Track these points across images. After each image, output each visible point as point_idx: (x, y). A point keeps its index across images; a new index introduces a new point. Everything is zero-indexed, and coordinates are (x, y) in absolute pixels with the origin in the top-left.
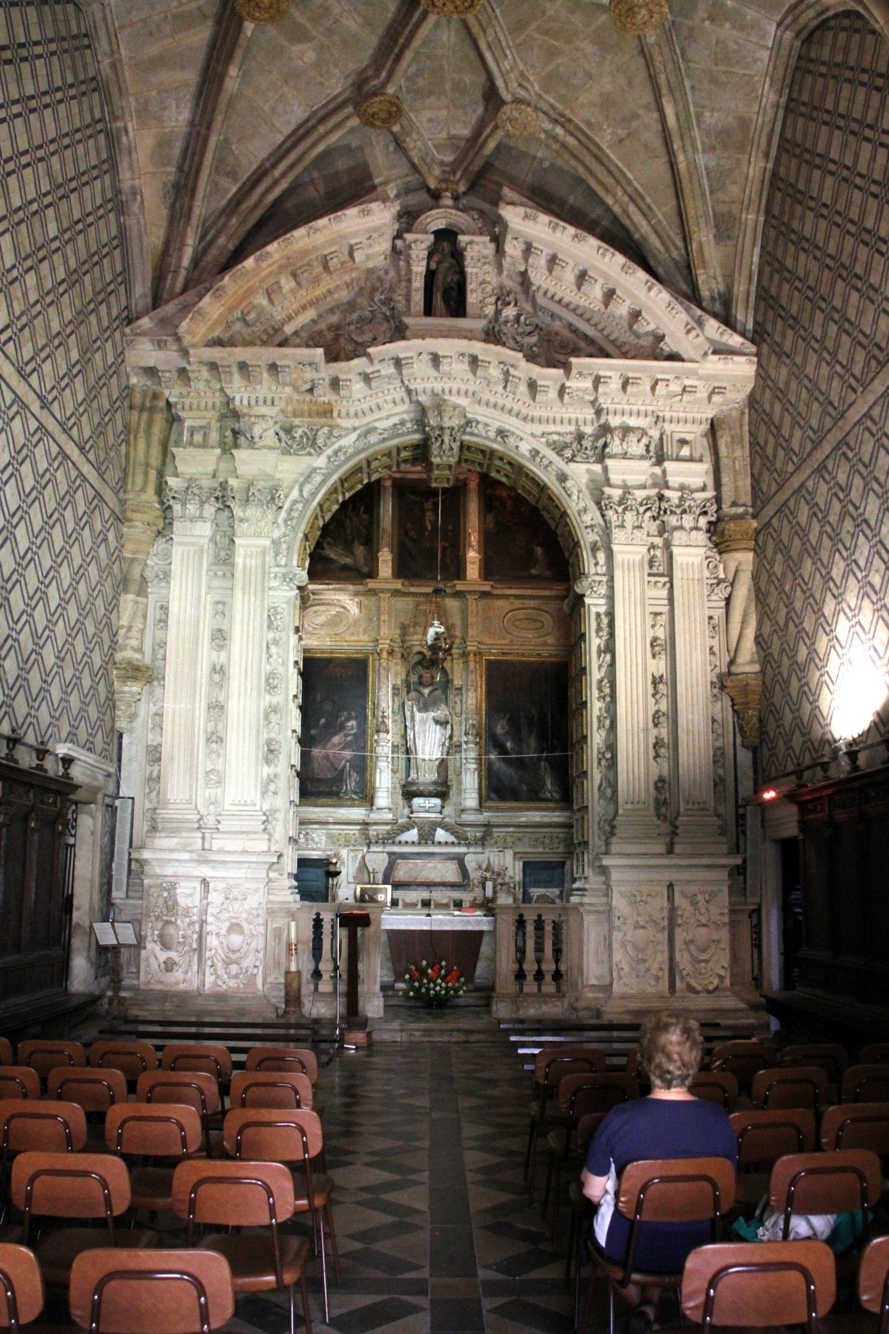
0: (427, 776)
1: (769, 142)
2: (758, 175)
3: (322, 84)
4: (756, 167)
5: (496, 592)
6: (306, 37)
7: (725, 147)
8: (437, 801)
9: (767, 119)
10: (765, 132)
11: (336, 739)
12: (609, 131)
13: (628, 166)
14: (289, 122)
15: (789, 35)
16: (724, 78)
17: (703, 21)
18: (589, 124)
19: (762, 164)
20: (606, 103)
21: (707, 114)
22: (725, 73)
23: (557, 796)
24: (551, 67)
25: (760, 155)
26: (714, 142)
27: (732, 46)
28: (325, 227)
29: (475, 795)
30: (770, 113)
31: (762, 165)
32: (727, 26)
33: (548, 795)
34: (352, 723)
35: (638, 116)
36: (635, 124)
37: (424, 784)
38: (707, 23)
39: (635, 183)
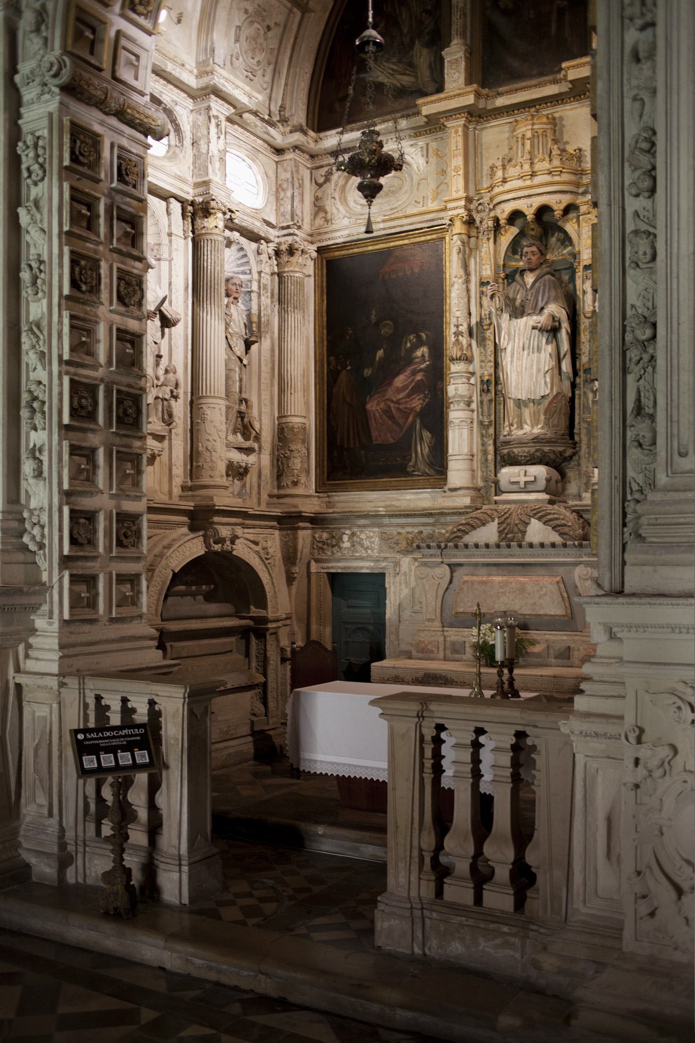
0: (528, 428)
8: (539, 471)
34: (423, 351)
37: (521, 443)
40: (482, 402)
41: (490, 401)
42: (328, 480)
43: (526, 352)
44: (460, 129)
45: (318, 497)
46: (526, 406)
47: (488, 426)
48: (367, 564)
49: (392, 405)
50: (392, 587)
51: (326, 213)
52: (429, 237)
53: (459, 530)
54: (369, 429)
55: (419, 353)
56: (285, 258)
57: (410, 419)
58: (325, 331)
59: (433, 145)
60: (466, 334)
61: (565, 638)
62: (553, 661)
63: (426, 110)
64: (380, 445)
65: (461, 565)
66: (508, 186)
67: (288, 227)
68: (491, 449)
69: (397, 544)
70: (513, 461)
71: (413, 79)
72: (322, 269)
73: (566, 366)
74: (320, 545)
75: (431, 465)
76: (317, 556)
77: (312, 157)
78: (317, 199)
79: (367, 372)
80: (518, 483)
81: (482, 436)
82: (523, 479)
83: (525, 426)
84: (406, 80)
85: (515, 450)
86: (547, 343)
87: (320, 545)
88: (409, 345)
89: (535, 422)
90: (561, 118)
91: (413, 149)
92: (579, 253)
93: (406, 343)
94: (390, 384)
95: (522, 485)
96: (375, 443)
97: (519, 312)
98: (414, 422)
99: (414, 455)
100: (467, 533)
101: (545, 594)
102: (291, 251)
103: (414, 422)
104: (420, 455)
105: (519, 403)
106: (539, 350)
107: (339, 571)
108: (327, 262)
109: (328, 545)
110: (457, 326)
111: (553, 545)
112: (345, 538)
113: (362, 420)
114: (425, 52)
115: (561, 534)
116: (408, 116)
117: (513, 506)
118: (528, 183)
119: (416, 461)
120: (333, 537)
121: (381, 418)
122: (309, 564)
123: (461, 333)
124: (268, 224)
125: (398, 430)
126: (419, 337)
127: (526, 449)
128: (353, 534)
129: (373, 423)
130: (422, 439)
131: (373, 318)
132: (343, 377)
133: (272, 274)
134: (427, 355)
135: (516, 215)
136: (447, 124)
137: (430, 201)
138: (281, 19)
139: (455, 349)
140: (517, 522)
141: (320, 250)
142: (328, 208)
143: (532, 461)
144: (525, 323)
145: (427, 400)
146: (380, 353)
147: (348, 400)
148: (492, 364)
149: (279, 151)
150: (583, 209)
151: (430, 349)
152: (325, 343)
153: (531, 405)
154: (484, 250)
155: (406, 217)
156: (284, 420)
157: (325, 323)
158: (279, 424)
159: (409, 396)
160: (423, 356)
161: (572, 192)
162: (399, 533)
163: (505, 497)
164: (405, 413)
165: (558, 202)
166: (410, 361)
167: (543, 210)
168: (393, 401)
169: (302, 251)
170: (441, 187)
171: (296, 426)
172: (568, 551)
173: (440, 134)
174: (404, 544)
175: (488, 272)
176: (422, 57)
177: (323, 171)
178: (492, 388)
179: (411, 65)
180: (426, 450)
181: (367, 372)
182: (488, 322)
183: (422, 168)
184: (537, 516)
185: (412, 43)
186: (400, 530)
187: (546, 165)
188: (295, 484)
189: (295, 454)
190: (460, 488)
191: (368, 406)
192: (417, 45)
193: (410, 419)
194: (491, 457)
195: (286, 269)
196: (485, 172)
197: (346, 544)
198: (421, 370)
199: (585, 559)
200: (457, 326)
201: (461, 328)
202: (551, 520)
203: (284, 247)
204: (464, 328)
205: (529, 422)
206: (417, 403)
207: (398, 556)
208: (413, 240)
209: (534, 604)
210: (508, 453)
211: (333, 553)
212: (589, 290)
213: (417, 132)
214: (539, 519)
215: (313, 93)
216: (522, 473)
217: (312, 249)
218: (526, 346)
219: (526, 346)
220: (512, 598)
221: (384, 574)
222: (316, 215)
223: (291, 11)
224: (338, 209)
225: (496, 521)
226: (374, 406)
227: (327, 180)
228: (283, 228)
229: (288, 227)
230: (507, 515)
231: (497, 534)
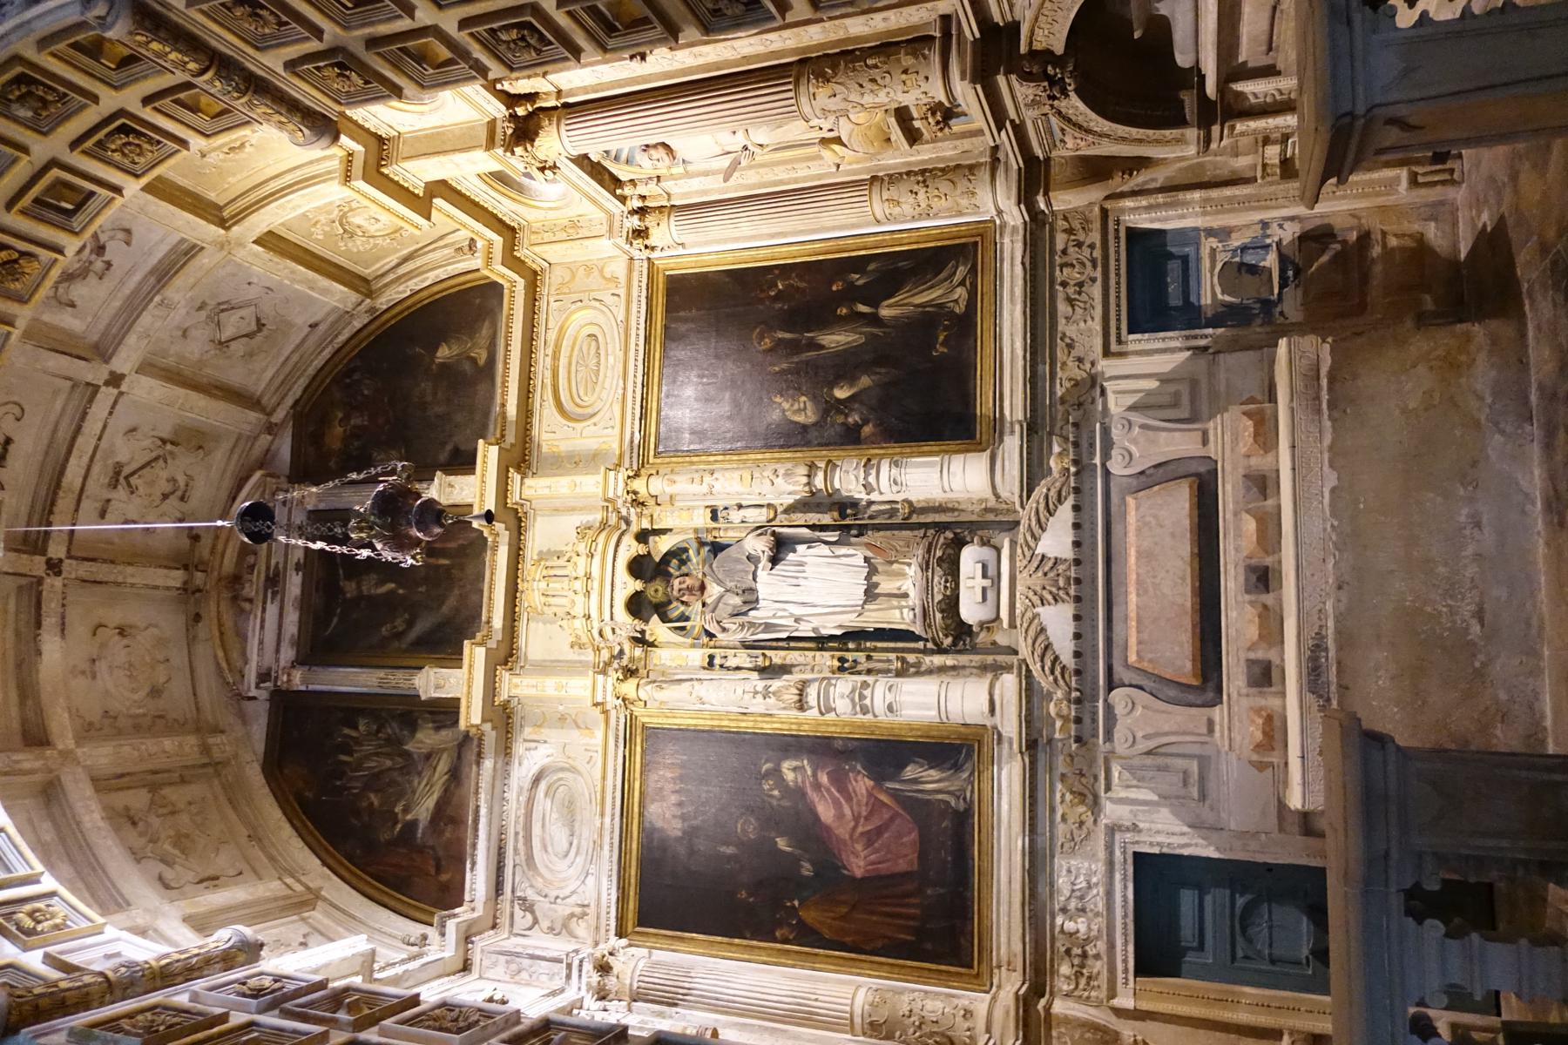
0: (907, 590)
5: (511, 438)
8: (970, 558)
11: (826, 812)
23: (962, 271)
29: (957, 461)
33: (961, 293)
37: (928, 588)
40: (869, 672)
41: (869, 658)
42: (972, 967)
43: (801, 582)
44: (516, 680)
45: (999, 987)
46: (876, 585)
47: (903, 660)
48: (1118, 886)
49: (860, 829)
50: (1160, 839)
51: (573, 915)
52: (639, 749)
53: (1052, 672)
54: (892, 876)
55: (790, 776)
56: (611, 982)
57: (884, 798)
58: (737, 941)
59: (528, 732)
60: (769, 682)
61: (1229, 487)
62: (1270, 502)
63: (476, 719)
64: (919, 857)
65: (1109, 669)
66: (594, 614)
67: (569, 966)
68: (938, 660)
69: (1082, 823)
70: (951, 604)
71: (445, 756)
72: (647, 934)
73: (832, 536)
74: (1083, 981)
75: (957, 768)
76: (1103, 994)
77: (494, 927)
78: (551, 929)
79: (807, 869)
80: (984, 590)
81: (918, 674)
82: (980, 582)
83: (904, 588)
84: (443, 766)
85: (938, 597)
86: (794, 551)
87: (1083, 981)
88: (776, 793)
89: (903, 575)
90: (540, 553)
91: (525, 762)
92: (696, 531)
93: (772, 796)
94: (828, 829)
95: (987, 583)
96: (915, 867)
97: (748, 597)
98: (888, 792)
99: (940, 797)
100: (1056, 658)
101: (1155, 517)
102: (604, 968)
103: (888, 792)
104: (941, 785)
105: (871, 594)
106: (801, 564)
107: (1131, 948)
108: (640, 924)
109: (1082, 966)
110: (756, 693)
111: (1076, 508)
112: (1070, 926)
113: (878, 887)
114: (419, 735)
115: (1060, 501)
116: (480, 755)
117: (1019, 588)
118: (596, 585)
119: (948, 793)
120: (1068, 952)
121: (877, 851)
122: (1119, 1012)
123: (767, 688)
124: (553, 994)
125: (897, 822)
126: (767, 775)
127: (936, 579)
128: (1064, 910)
129: (884, 868)
130: (915, 781)
131: (730, 850)
132: (810, 916)
133: (630, 1010)
134: (795, 763)
135: (636, 605)
136: (504, 696)
137: (593, 741)
138: (305, 929)
139: (786, 697)
140: (1040, 574)
141: (620, 934)
142: (568, 911)
143: (952, 567)
144: (768, 583)
145: (859, 767)
146: (782, 843)
147: (844, 910)
148: (818, 654)
149: (466, 967)
150: (646, 524)
151: (787, 758)
152: (755, 943)
153: (875, 579)
154: (669, 663)
155: (604, 778)
156: (858, 1020)
157: (725, 940)
158: (864, 1034)
159: (849, 799)
160: (794, 769)
161: (623, 534)
162: (1064, 818)
163: (1004, 614)
164: (876, 806)
165: (630, 548)
166: (799, 793)
167: (638, 567)
168: (854, 828)
169: (611, 954)
170: (580, 722)
171: (870, 998)
172: (1086, 487)
173: (516, 719)
174: (1082, 809)
175: (698, 656)
176: (426, 738)
177: (518, 913)
178: (850, 656)
179: (428, 757)
180: (934, 774)
181: (807, 869)
182: (761, 659)
183: (550, 751)
184: (1032, 544)
185: (408, 755)
186: (1058, 817)
187: (582, 561)
188: (968, 1014)
189: (917, 1006)
190: (991, 695)
191: (859, 873)
192: (408, 747)
193: (884, 798)
194: (949, 660)
195: (628, 982)
196: (576, 658)
197: (1080, 925)
198: (815, 775)
199: (1097, 460)
200: (756, 693)
201: (759, 688)
202: (1039, 521)
203: (596, 978)
204: (760, 685)
205: (898, 584)
206: (862, 784)
207: (1104, 821)
208: (638, 775)
209: (1173, 535)
210: (942, 611)
211: (1097, 957)
212: (742, 512)
213: (505, 751)
214: (1036, 539)
215: (418, 915)
216: (970, 583)
217: (615, 942)
218: (795, 581)
219: (795, 581)
220: (1163, 574)
221: (1136, 854)
222: (572, 935)
223: (303, 919)
224: (573, 892)
225: (1039, 610)
226: (858, 863)
227: (528, 907)
228: (569, 977)
229: (569, 966)
230: (1031, 594)
231: (1060, 605)
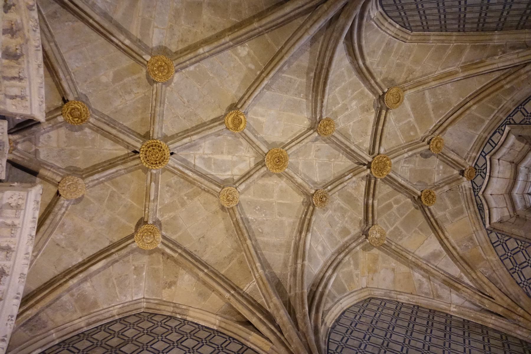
1: (95, 322)
2: (76, 327)
3: (86, 81)
4: (81, 323)
6: (114, 81)
7: (76, 301)
9: (104, 315)
10: (98, 317)
12: (62, 237)
13: (44, 253)
14: (70, 58)
15: (144, 305)
16: (110, 285)
17: (133, 265)
18: (63, 224)
19: (83, 324)
20: (78, 232)
21: (89, 284)
22: (113, 283)
24: (92, 200)
25: (87, 321)
26: (76, 294)
27: (127, 282)
28: (38, 72)
30: (107, 315)
31: (83, 324)
32: (135, 277)
35: (76, 250)
36: (71, 249)
38: (133, 267)
39: (36, 260)
